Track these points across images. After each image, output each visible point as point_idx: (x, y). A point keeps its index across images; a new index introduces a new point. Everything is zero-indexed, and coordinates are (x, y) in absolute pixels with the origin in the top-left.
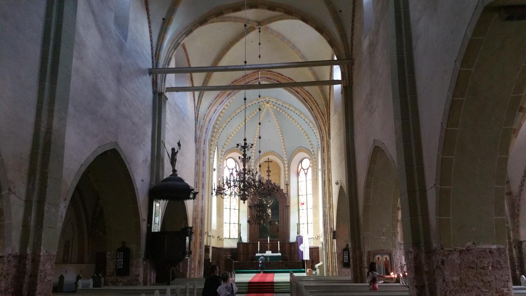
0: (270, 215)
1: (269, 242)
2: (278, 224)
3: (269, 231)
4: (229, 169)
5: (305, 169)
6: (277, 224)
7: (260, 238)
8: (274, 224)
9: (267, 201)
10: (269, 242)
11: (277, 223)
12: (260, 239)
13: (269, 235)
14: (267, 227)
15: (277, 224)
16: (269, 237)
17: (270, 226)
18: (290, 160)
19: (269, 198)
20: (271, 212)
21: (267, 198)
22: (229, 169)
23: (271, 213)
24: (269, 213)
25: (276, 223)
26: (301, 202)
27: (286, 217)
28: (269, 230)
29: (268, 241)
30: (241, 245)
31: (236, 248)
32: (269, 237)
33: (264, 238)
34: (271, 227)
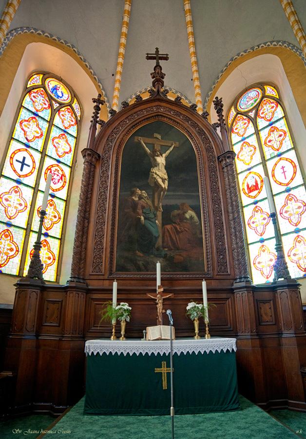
0: (165, 185)
1: (159, 283)
2: (196, 218)
3: (160, 240)
4: (51, 98)
5: (251, 111)
6: (191, 218)
7: (121, 268)
8: (182, 218)
9: (154, 144)
10: (159, 283)
11: (190, 213)
12: (124, 275)
13: (161, 259)
14: (148, 224)
15: (191, 218)
16: (158, 265)
17: (163, 224)
18: (207, 99)
19: (159, 137)
20: (166, 177)
21: (152, 136)
22: (51, 98)
23: (166, 182)
24: (160, 181)
25: (187, 216)
26: (246, 188)
27: (225, 195)
28: (160, 240)
29: (155, 279)
30: (33, 296)
31: (12, 308)
32: (158, 265)
33: (139, 269)
34: (169, 227)
